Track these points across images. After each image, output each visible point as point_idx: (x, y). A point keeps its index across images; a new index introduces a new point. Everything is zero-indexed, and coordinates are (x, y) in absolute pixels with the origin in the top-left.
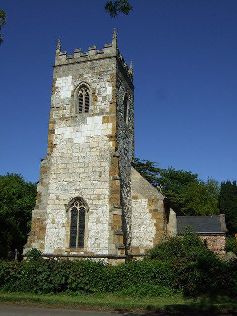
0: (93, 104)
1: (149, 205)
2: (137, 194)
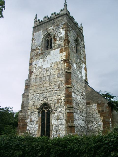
0: (54, 43)
2: (89, 101)
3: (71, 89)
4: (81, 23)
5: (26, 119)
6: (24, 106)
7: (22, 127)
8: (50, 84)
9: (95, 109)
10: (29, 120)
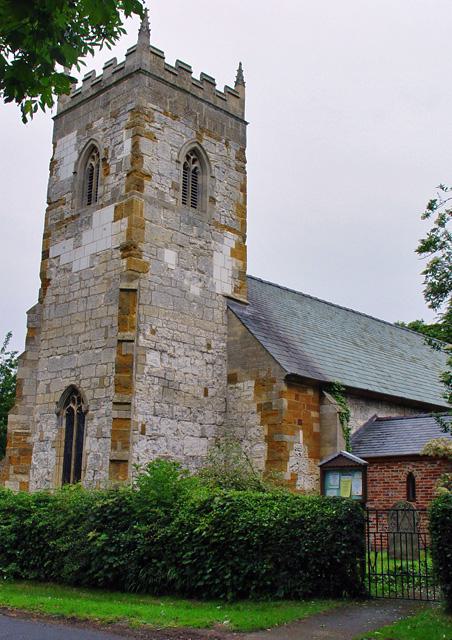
1: (257, 393)
2: (235, 371)
3: (129, 344)
4: (240, 64)
5: (28, 435)
6: (24, 393)
7: (19, 458)
8: (86, 326)
9: (250, 399)
10: (37, 437)
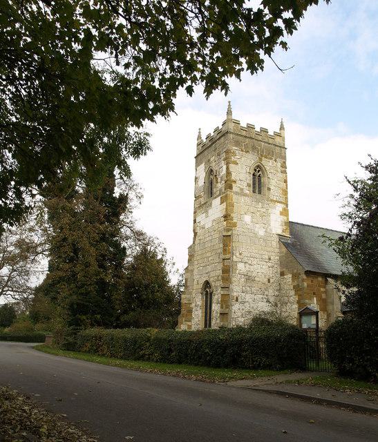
1: (293, 280)
5: (191, 304)
